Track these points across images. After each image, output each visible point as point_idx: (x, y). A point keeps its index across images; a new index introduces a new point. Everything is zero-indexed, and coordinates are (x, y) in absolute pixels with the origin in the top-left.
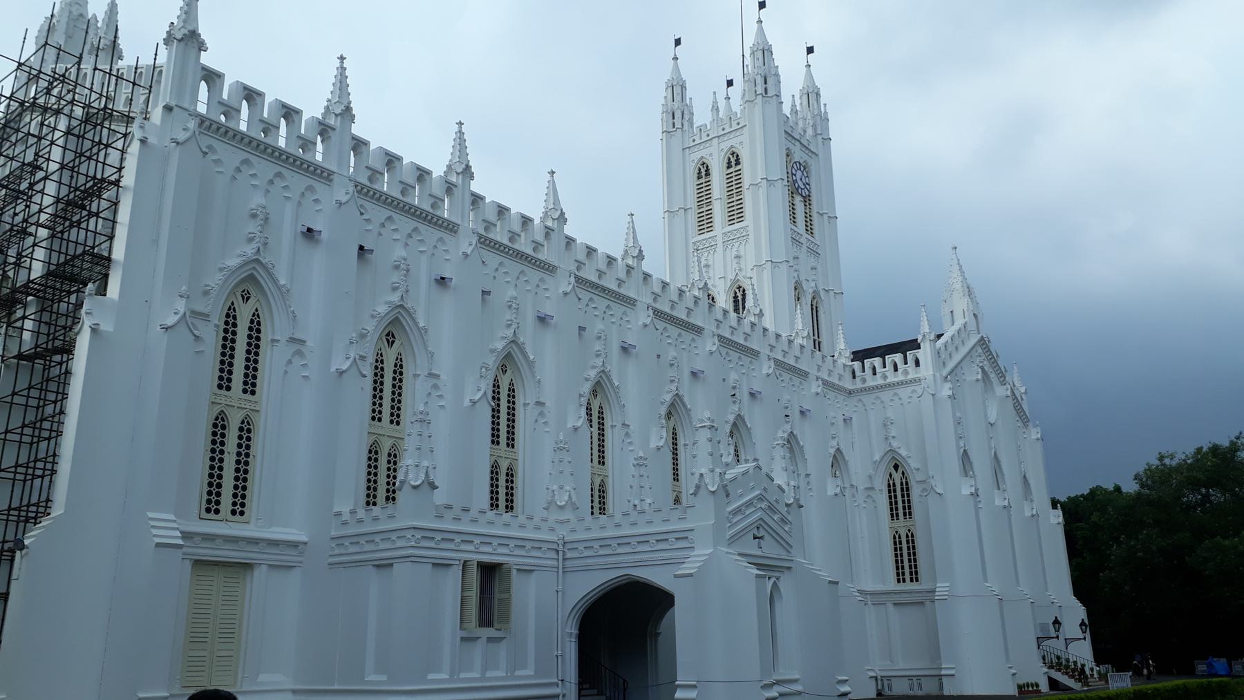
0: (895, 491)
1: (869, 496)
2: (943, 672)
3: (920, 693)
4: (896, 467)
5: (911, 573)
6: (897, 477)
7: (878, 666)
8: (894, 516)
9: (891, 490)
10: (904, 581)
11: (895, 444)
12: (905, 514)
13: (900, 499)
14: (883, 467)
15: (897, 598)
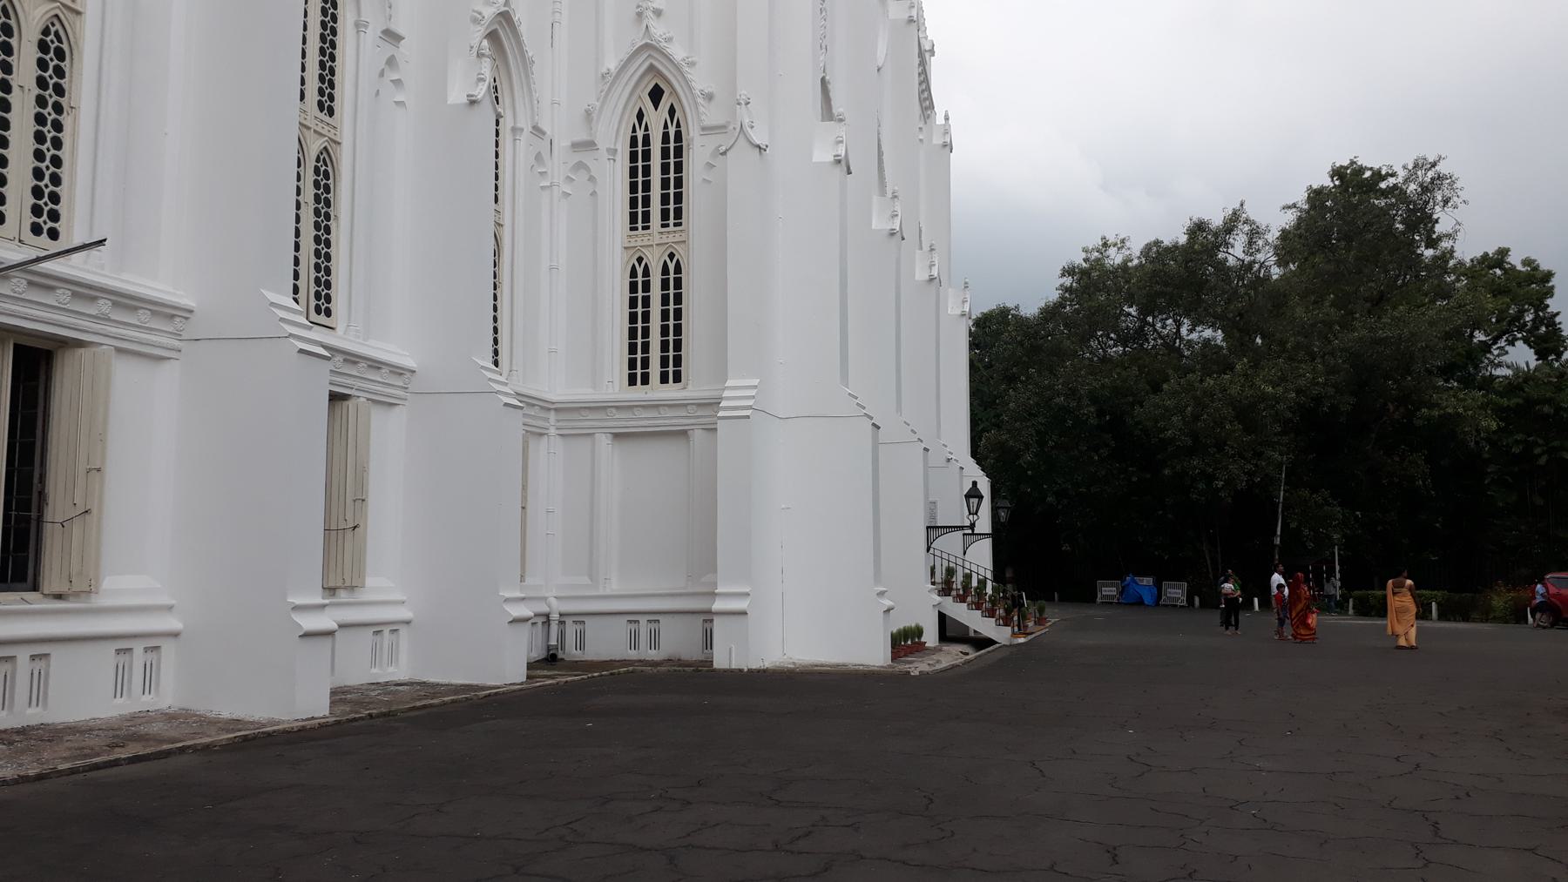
0: (647, 156)
1: (580, 166)
2: (718, 605)
3: (653, 655)
4: (656, 95)
5: (664, 362)
6: (656, 120)
7: (555, 585)
8: (638, 218)
9: (638, 152)
10: (645, 380)
11: (659, 29)
12: (665, 215)
13: (657, 177)
14: (622, 92)
15: (624, 422)
